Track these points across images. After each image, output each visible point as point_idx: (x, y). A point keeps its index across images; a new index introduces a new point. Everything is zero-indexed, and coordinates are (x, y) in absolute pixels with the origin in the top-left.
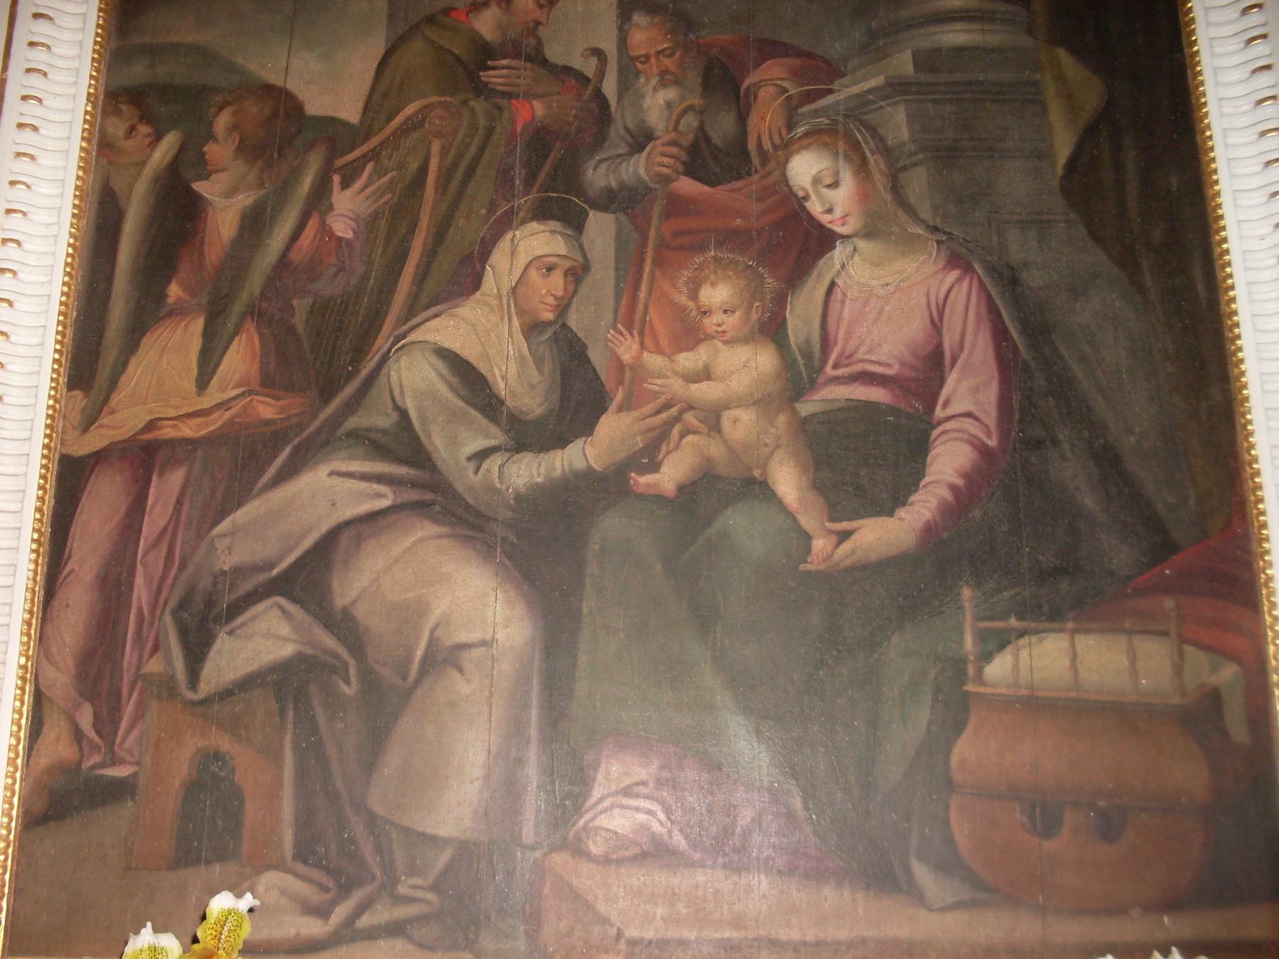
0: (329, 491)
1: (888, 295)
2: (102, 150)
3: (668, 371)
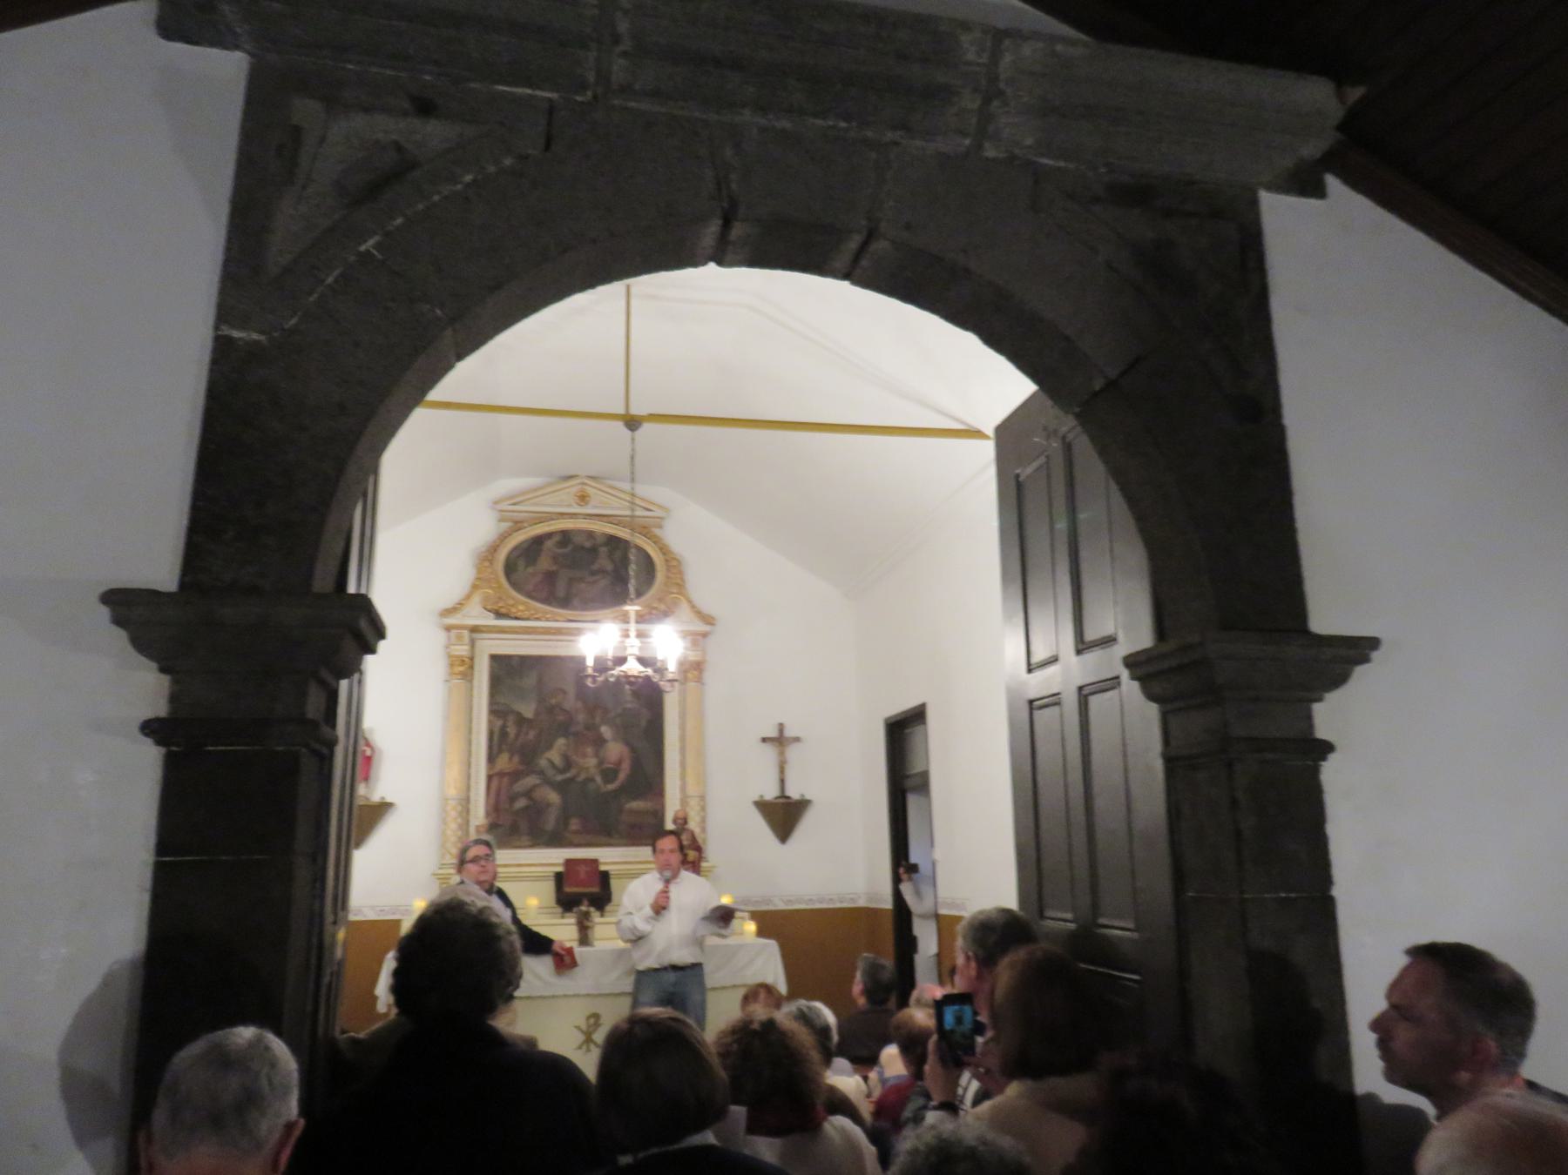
0: (531, 780)
1: (615, 750)
2: (490, 722)
3: (581, 761)
